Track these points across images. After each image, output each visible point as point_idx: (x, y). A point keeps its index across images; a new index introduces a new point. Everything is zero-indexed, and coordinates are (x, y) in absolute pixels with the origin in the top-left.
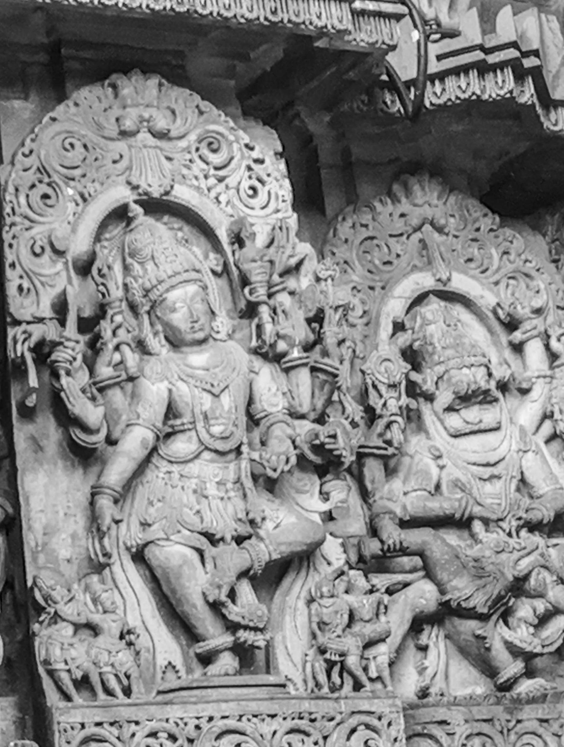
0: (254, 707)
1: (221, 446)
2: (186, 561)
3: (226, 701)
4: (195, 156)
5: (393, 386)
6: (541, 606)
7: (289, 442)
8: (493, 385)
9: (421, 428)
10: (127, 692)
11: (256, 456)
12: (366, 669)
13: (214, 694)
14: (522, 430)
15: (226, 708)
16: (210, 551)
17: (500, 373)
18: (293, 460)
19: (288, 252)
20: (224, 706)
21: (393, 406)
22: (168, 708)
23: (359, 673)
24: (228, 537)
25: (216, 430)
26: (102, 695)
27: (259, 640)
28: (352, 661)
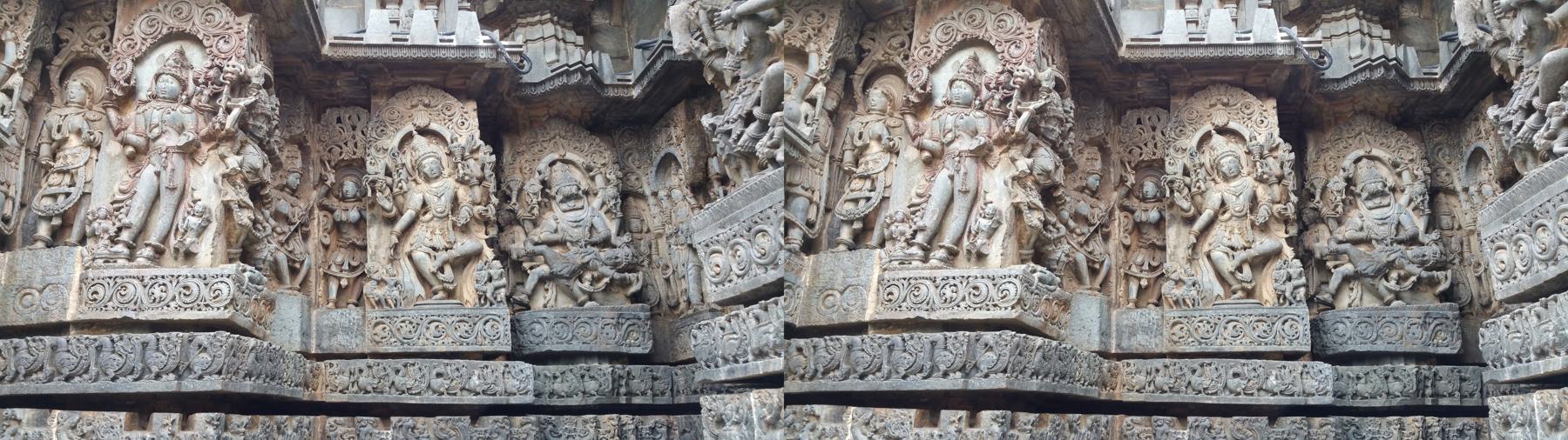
5: (535, 194)
6: (596, 274)
8: (580, 192)
9: (551, 209)
12: (495, 299)
14: (593, 209)
15: (432, 312)
16: (433, 253)
17: (584, 186)
21: (535, 201)
23: (492, 299)
27: (451, 287)
28: (488, 295)
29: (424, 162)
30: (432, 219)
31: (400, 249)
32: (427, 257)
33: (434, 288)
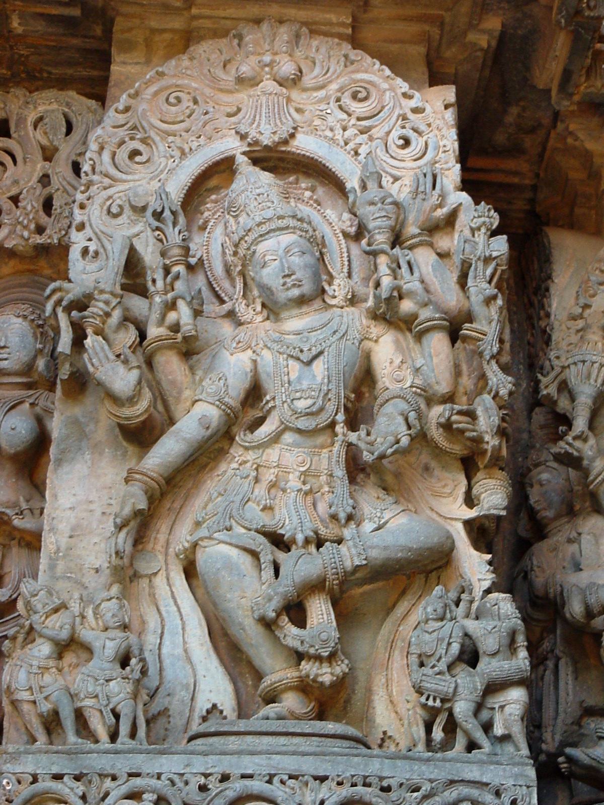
0: (290, 764)
1: (302, 424)
2: (229, 565)
3: (252, 753)
4: (333, 105)
7: (400, 419)
10: (114, 737)
11: (353, 437)
13: (233, 743)
15: (249, 764)
18: (405, 441)
19: (434, 199)
20: (247, 759)
22: (164, 759)
24: (300, 538)
25: (301, 405)
26: (72, 738)
29: (261, 248)
30: (276, 438)
31: (160, 533)
32: (246, 560)
33: (267, 682)
